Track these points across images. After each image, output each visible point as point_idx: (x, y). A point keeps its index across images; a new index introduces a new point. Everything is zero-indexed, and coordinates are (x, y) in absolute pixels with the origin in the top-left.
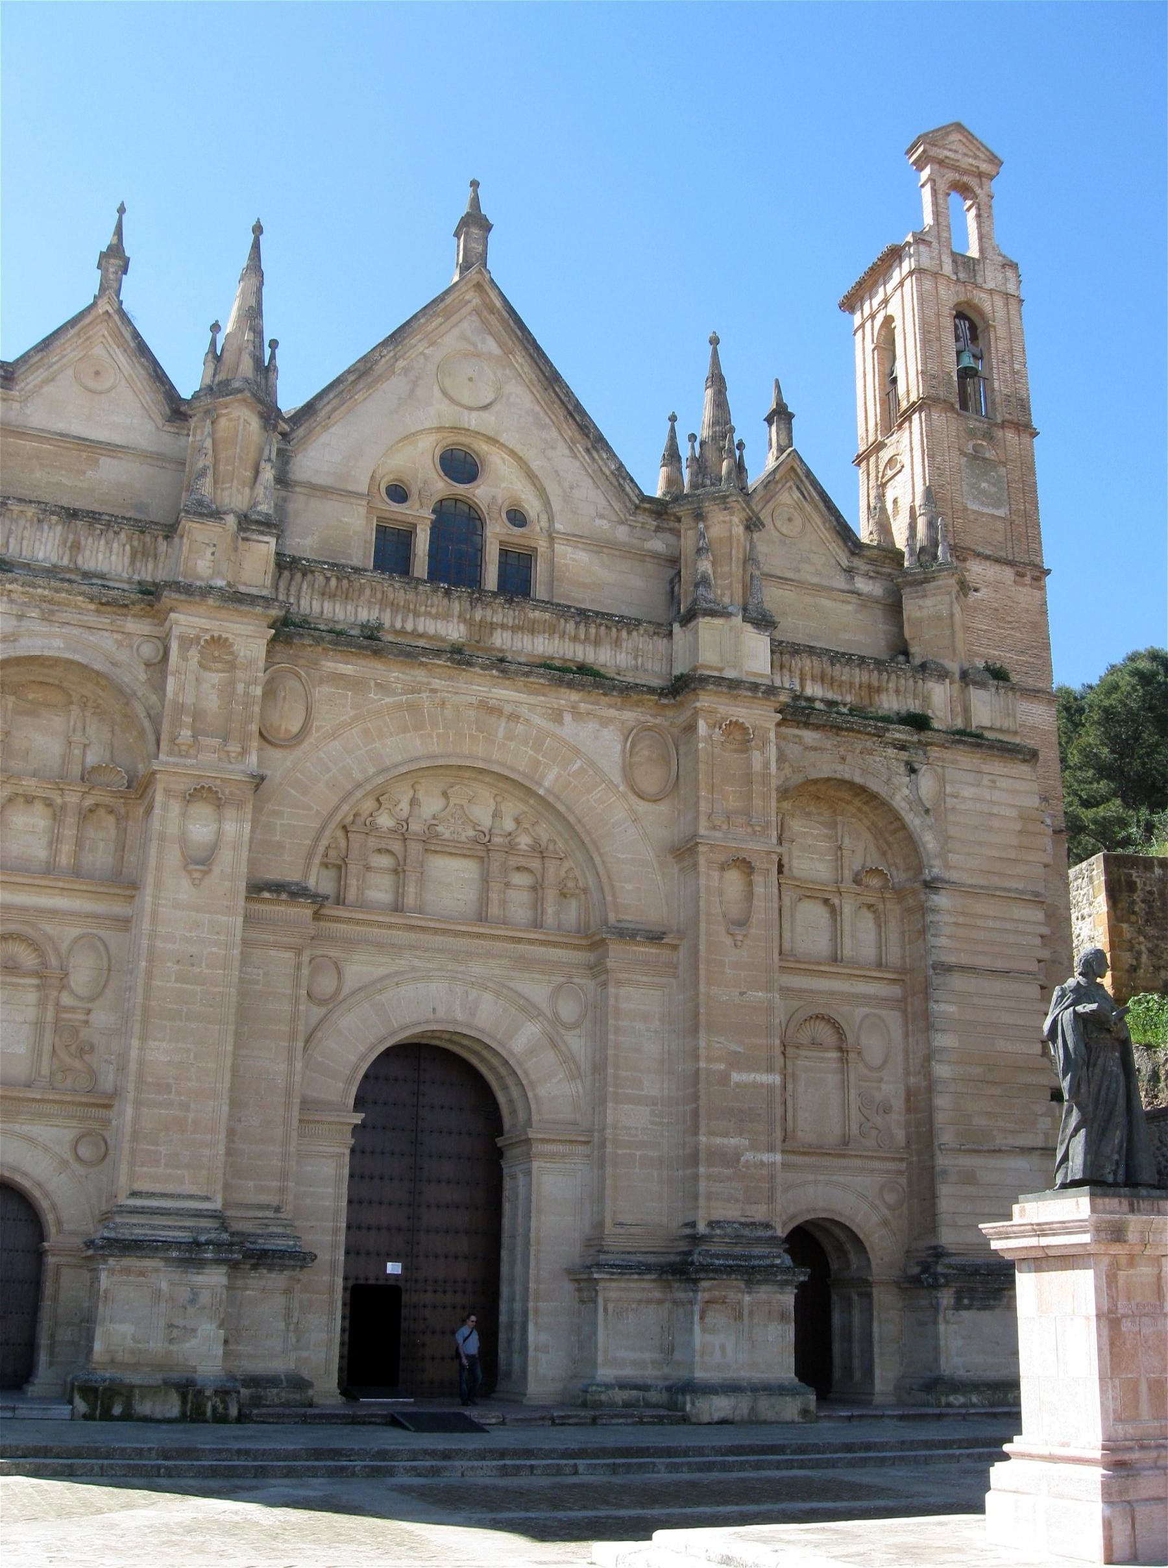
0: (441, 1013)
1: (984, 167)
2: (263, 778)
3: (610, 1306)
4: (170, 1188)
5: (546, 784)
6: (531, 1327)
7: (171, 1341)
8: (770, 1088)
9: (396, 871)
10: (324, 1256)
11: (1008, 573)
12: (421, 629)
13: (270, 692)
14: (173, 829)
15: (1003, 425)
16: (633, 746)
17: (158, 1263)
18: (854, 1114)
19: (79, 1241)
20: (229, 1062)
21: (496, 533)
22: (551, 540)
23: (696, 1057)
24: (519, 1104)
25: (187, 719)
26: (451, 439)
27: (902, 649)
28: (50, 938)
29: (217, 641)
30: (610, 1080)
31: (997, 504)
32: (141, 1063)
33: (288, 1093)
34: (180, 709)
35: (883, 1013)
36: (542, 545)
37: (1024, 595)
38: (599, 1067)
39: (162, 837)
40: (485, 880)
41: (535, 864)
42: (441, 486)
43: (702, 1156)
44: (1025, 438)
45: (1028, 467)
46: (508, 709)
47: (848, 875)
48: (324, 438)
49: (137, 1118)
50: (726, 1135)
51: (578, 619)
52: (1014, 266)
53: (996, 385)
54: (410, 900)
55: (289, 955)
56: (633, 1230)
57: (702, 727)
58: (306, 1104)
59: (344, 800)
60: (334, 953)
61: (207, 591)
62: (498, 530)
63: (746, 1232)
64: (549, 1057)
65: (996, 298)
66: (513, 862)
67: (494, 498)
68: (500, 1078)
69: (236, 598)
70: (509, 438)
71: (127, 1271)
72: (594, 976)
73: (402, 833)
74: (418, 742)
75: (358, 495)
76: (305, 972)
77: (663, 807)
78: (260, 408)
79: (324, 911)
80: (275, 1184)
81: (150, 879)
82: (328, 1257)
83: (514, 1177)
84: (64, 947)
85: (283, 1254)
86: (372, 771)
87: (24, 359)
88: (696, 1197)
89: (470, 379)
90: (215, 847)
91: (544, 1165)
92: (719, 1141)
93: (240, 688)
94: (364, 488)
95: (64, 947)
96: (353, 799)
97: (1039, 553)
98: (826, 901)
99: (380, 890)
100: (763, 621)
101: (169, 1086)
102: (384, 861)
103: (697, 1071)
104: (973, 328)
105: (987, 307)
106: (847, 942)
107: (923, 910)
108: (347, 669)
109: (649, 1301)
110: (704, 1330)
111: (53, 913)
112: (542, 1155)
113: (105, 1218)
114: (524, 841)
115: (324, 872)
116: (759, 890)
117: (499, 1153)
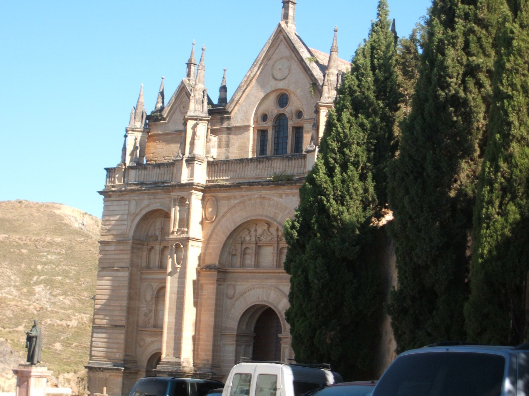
5: (278, 220)
26: (279, 92)
46: (267, 197)
51: (288, 159)
55: (212, 286)
67: (291, 111)
89: (280, 69)
91: (285, 345)
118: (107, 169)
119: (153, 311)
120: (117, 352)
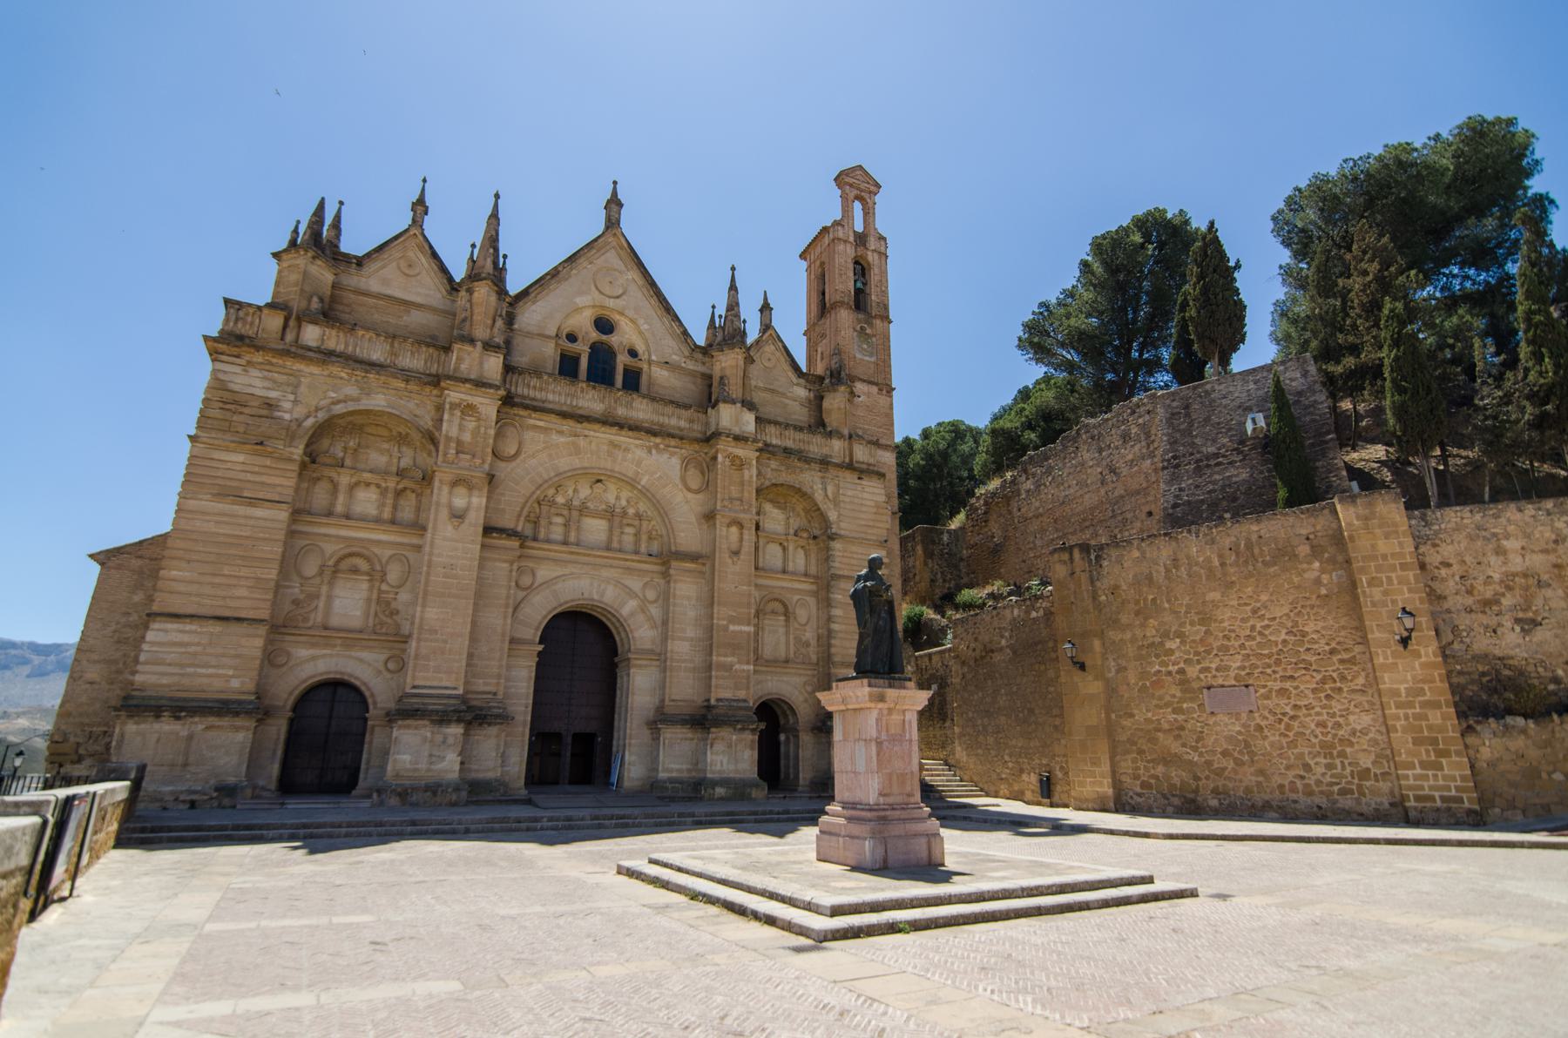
0: (586, 596)
1: (872, 188)
2: (493, 476)
3: (667, 741)
4: (435, 683)
5: (643, 483)
6: (627, 753)
7: (431, 763)
8: (749, 633)
9: (565, 525)
10: (519, 718)
11: (875, 389)
12: (580, 405)
13: (499, 435)
14: (444, 500)
15: (875, 317)
16: (686, 466)
17: (426, 722)
18: (792, 646)
19: (384, 712)
20: (470, 620)
21: (622, 360)
22: (650, 364)
23: (712, 618)
24: (625, 641)
25: (453, 445)
26: (601, 312)
27: (821, 423)
28: (376, 555)
29: (470, 407)
30: (670, 629)
31: (871, 356)
32: (422, 619)
33: (503, 635)
34: (449, 439)
35: (808, 598)
36: (645, 367)
37: (882, 400)
38: (665, 623)
39: (438, 504)
40: (611, 530)
41: (636, 523)
42: (595, 335)
43: (714, 667)
44: (886, 324)
45: (887, 338)
47: (792, 531)
48: (534, 307)
49: (418, 648)
50: (726, 656)
52: (884, 239)
53: (873, 297)
54: (572, 538)
55: (505, 565)
56: (680, 703)
57: (720, 456)
58: (513, 641)
59: (537, 489)
60: (531, 565)
61: (466, 381)
62: (623, 358)
63: (735, 704)
64: (641, 617)
65: (875, 254)
66: (625, 521)
68: (616, 628)
69: (480, 384)
70: (630, 313)
71: (408, 727)
72: (664, 578)
73: (569, 505)
74: (577, 461)
75: (549, 337)
76: (514, 573)
77: (700, 496)
78: (496, 288)
79: (527, 544)
80: (495, 681)
81: (430, 526)
82: (522, 718)
83: (622, 678)
84: (384, 561)
85: (497, 716)
86: (553, 474)
87: (369, 255)
88: (710, 687)
90: (467, 510)
92: (722, 659)
93: (482, 430)
94: (554, 334)
95: (384, 561)
96: (542, 489)
97: (891, 380)
98: (781, 544)
99: (557, 533)
100: (749, 405)
101: (436, 632)
102: (559, 520)
103: (712, 625)
104: (863, 269)
105: (870, 258)
106: (791, 564)
107: (828, 549)
108: (541, 424)
109: (686, 739)
110: (712, 753)
111: (379, 542)
112: (636, 666)
113: (400, 700)
114: (631, 511)
115: (527, 524)
116: (746, 537)
117: (615, 666)
118: (227, 302)
119: (323, 599)
120: (232, 677)
